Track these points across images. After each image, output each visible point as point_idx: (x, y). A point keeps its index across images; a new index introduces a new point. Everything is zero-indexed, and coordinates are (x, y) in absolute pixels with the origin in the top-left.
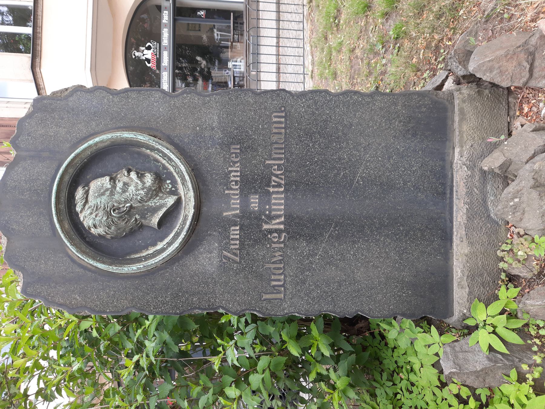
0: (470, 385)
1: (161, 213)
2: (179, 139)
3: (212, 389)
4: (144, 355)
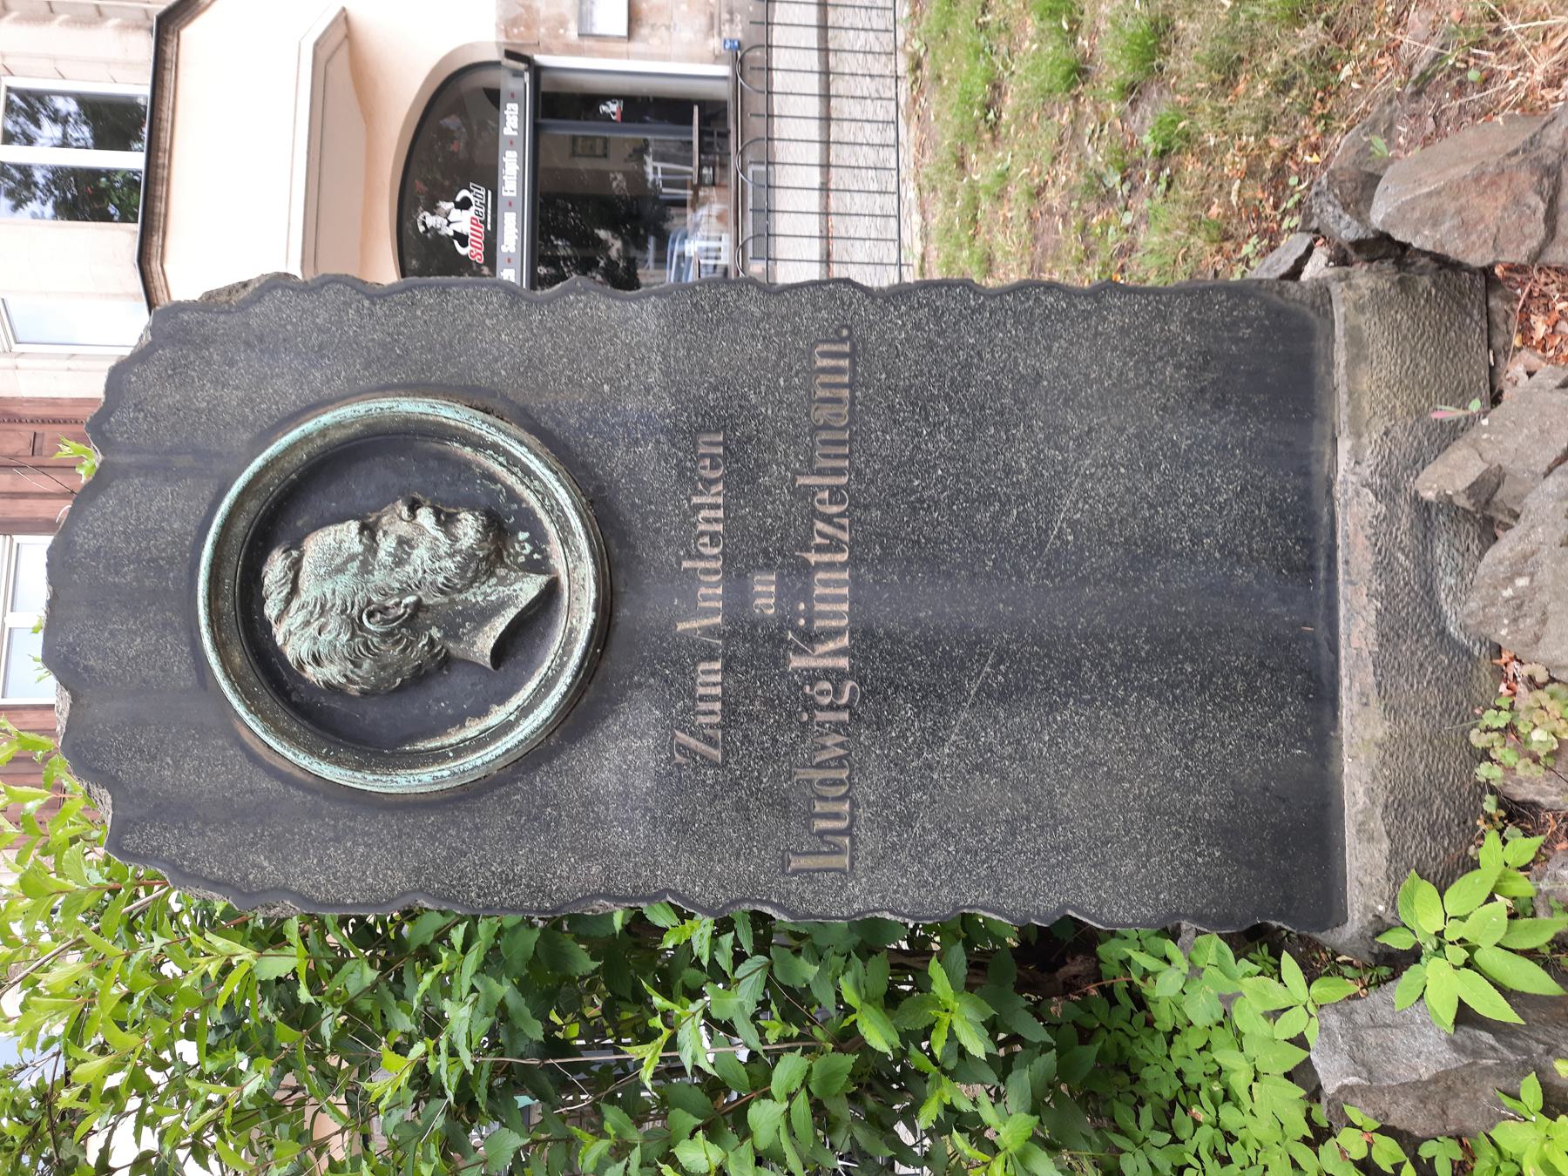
0: (1401, 1126)
1: (500, 624)
2: (553, 419)
3: (638, 1150)
4: (443, 1046)
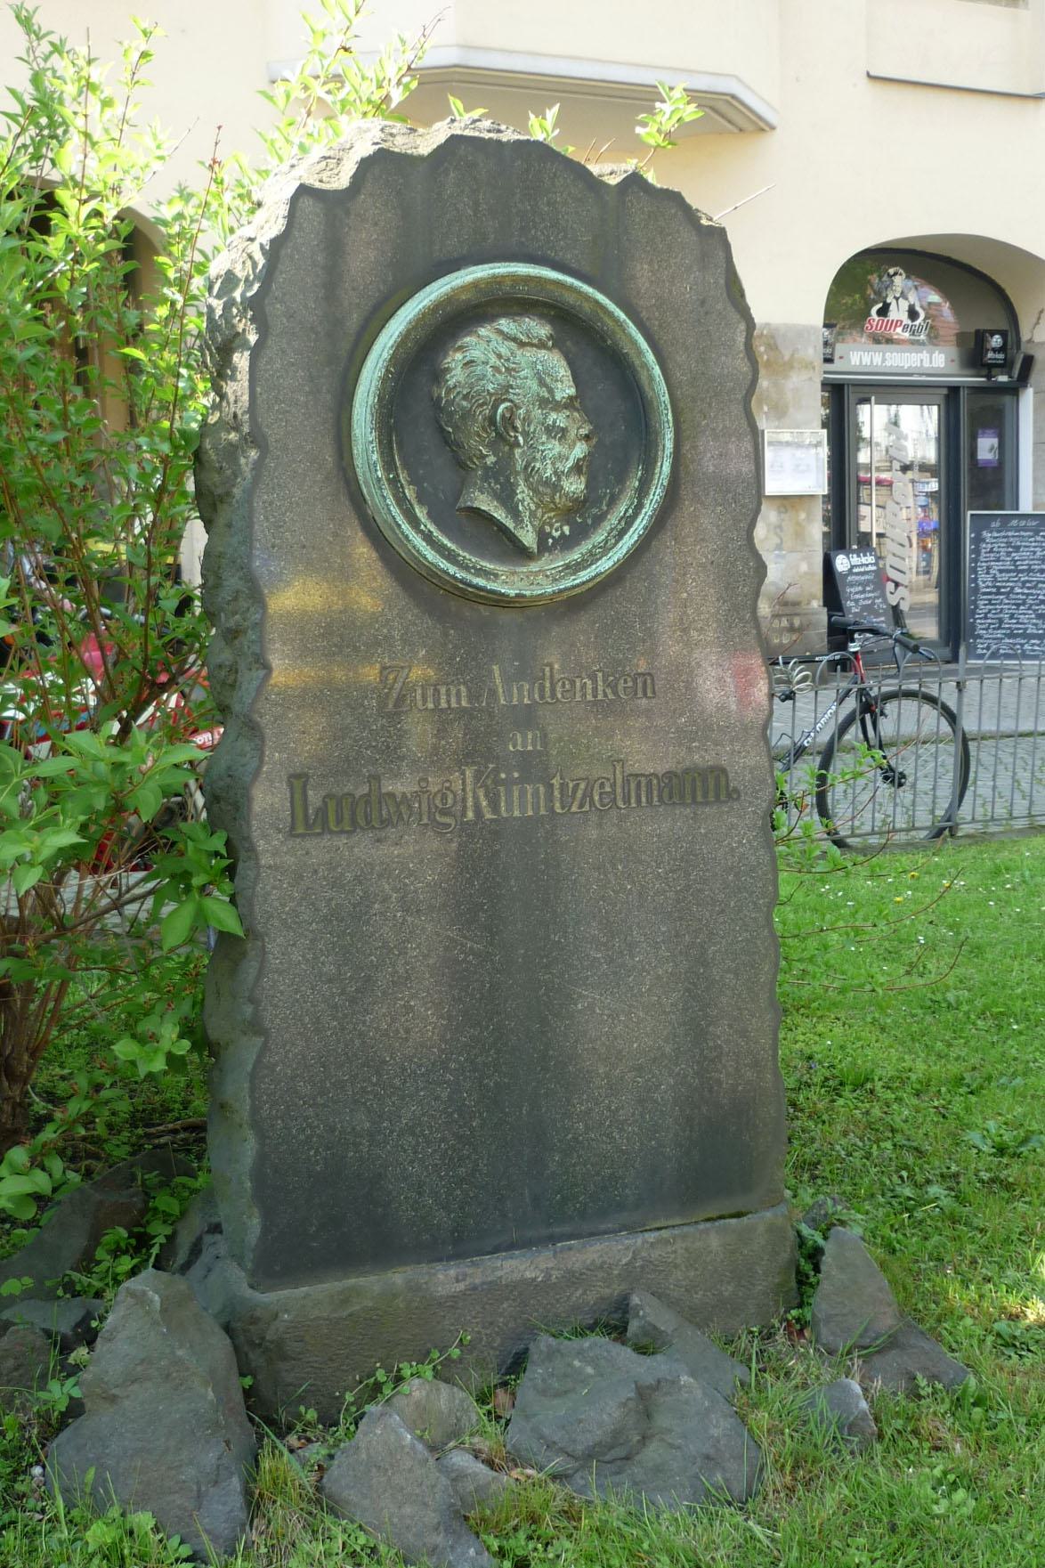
1: (500, 514)
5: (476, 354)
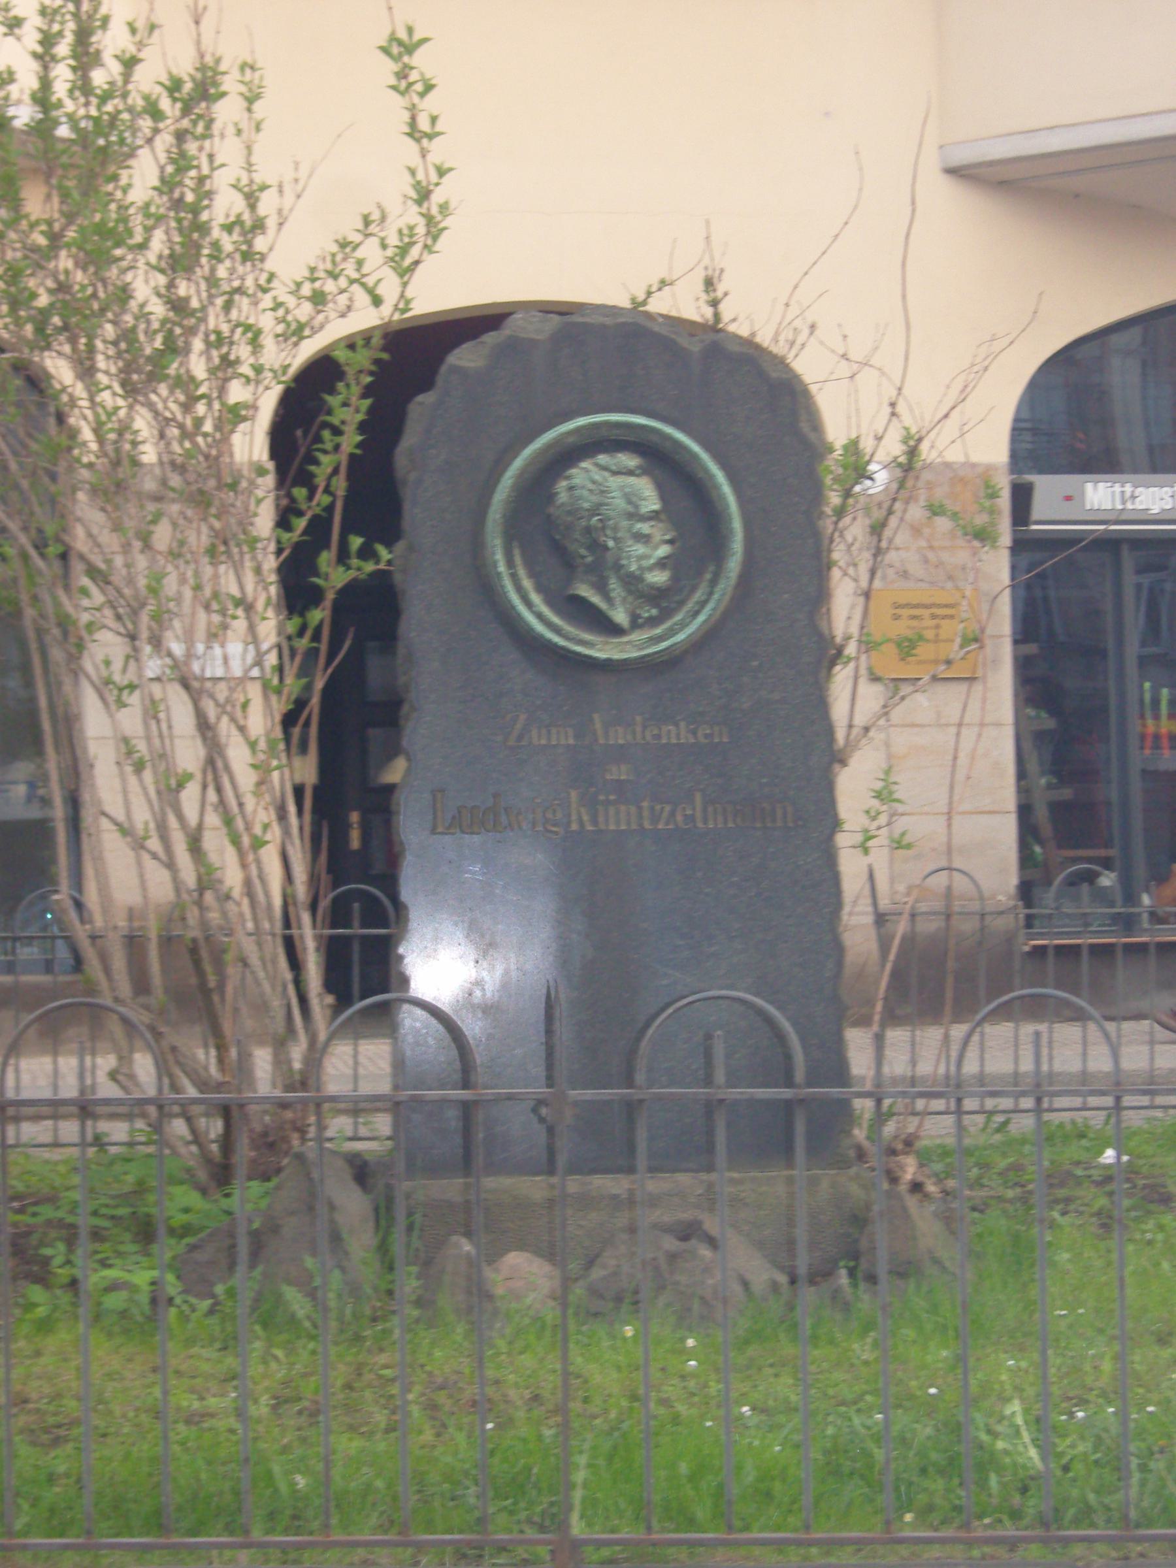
1: (596, 600)
5: (577, 481)
